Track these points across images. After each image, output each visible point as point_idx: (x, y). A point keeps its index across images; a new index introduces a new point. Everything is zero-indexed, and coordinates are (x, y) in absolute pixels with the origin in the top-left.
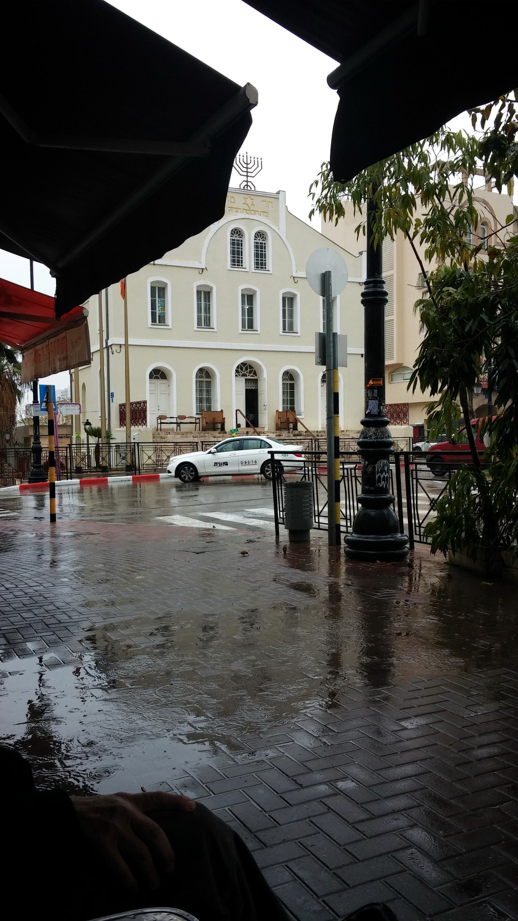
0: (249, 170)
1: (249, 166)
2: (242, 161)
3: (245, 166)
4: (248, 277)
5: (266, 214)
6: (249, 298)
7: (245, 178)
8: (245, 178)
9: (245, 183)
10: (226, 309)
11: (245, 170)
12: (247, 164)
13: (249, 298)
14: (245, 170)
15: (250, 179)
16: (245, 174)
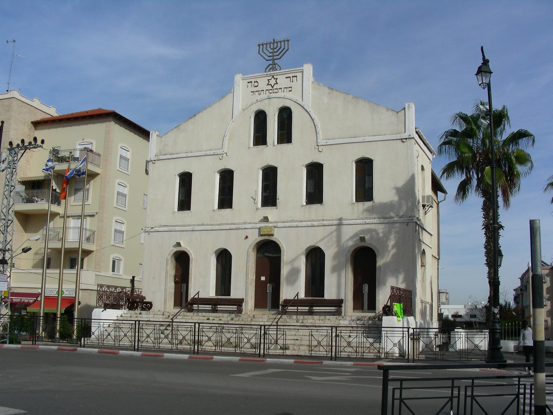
0: (275, 54)
1: (275, 50)
2: (268, 49)
3: (271, 51)
4: (273, 153)
5: (290, 89)
6: (270, 175)
7: (271, 62)
8: (271, 62)
9: (271, 66)
10: (248, 187)
11: (272, 54)
12: (273, 49)
13: (270, 175)
14: (272, 54)
15: (276, 61)
16: (271, 58)
